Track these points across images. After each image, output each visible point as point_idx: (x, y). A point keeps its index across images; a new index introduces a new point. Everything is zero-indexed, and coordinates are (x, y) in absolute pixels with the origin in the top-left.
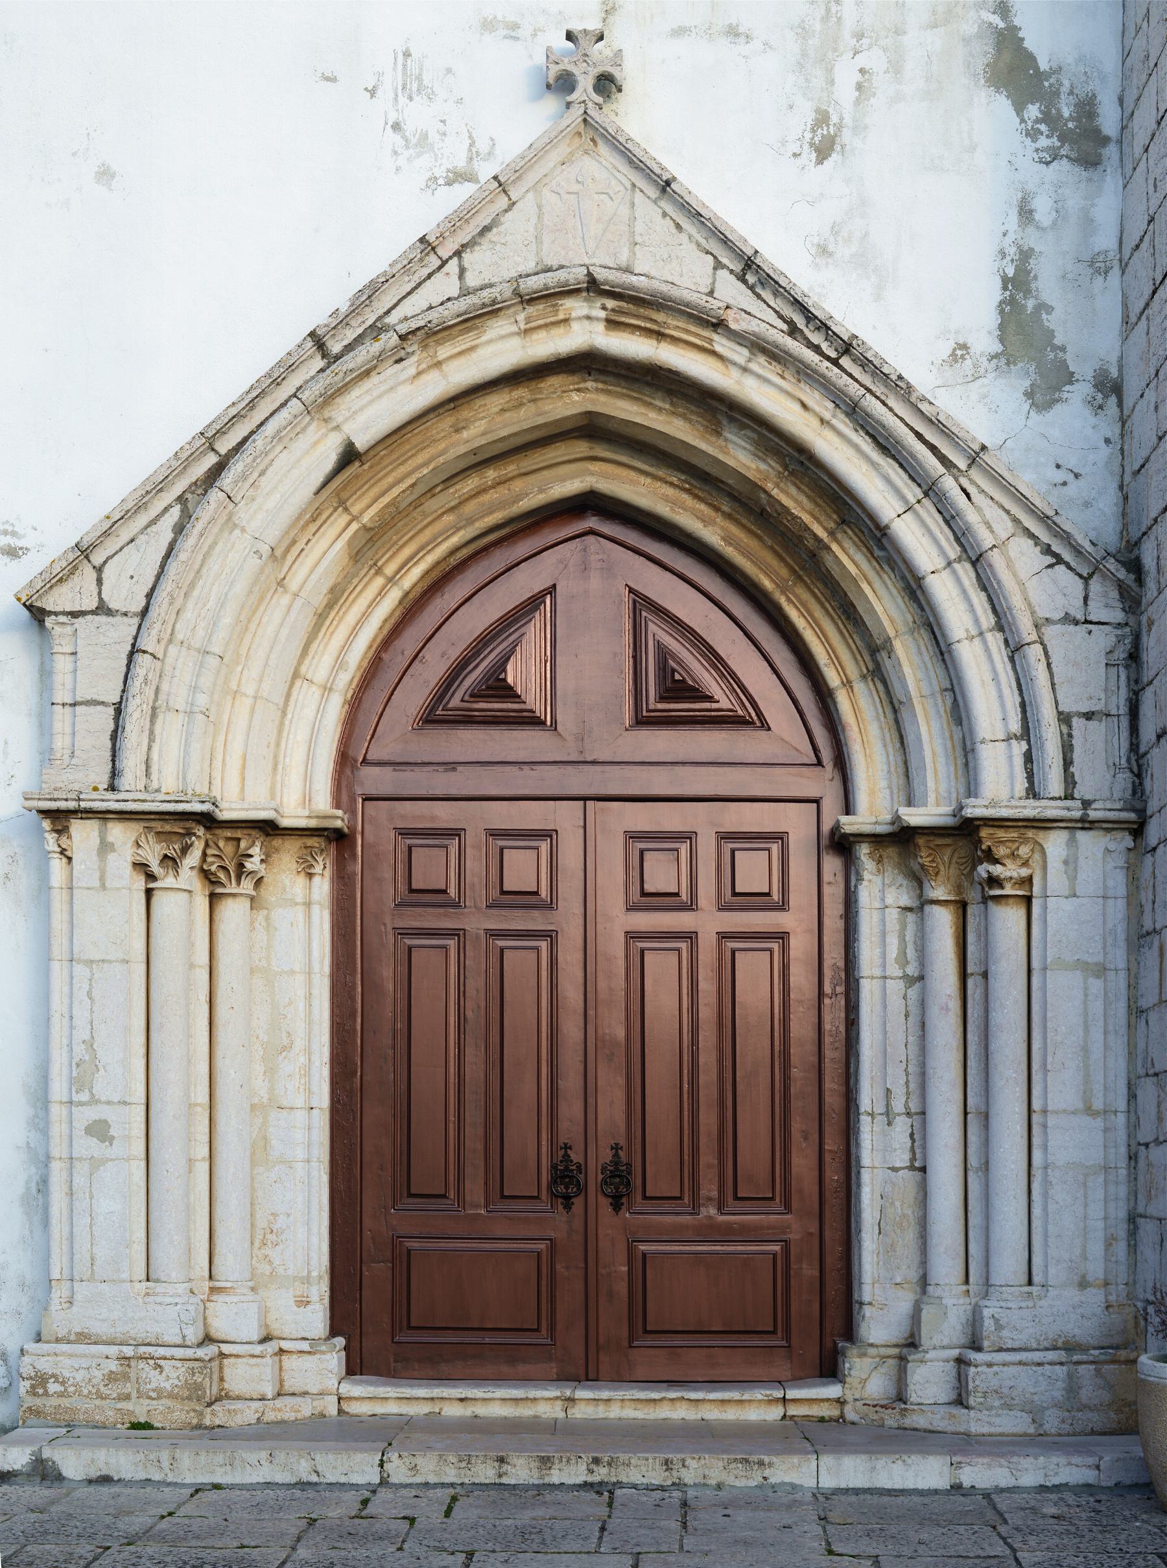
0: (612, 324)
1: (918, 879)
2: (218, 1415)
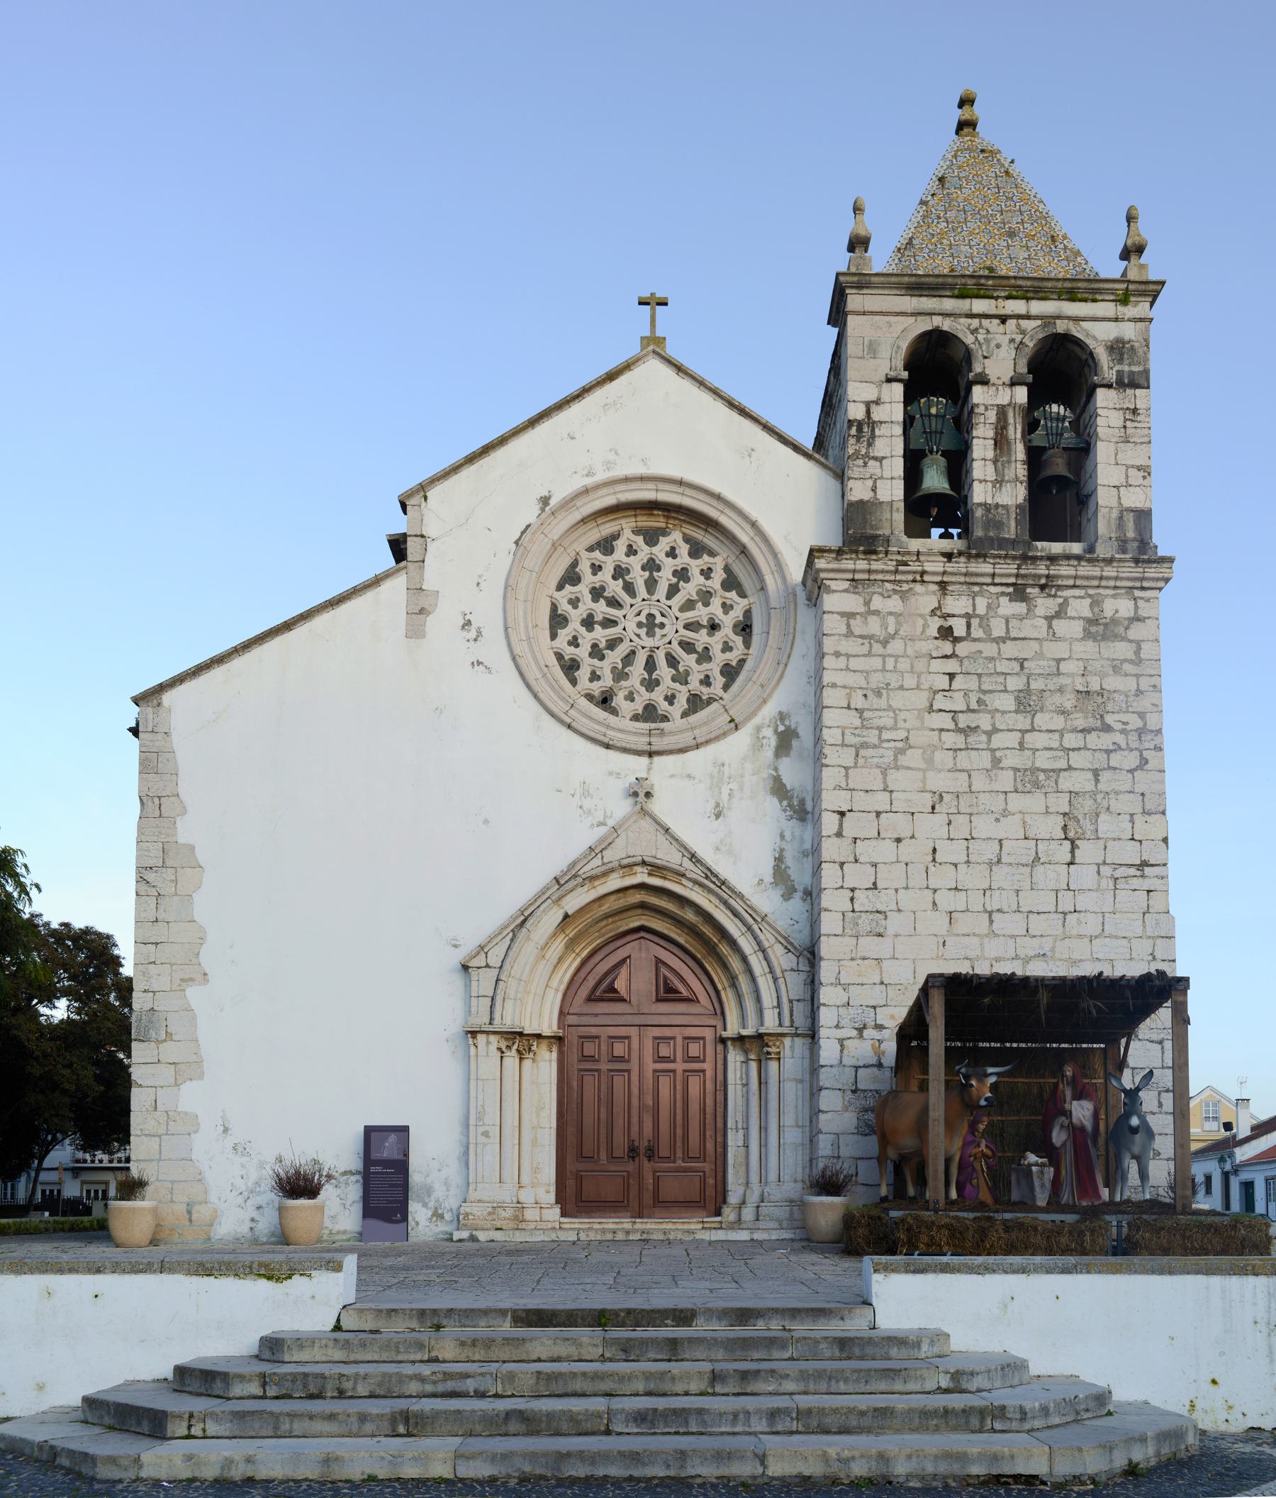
0: (650, 874)
1: (746, 1052)
2: (523, 1225)
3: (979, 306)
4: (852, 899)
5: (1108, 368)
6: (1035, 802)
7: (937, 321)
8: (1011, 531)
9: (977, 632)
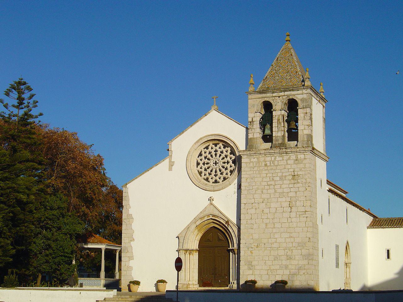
3: (274, 95)
6: (284, 199)
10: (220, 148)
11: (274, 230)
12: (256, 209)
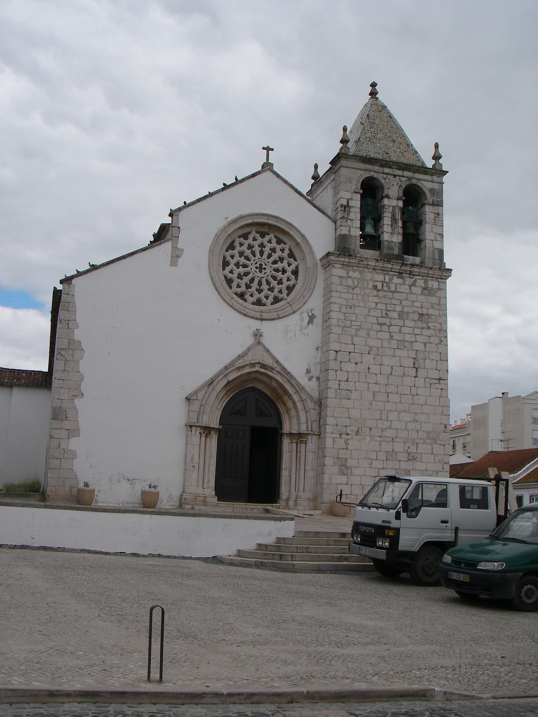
0: (260, 368)
3: (387, 170)
4: (339, 385)
5: (430, 199)
6: (404, 353)
7: (372, 174)
8: (396, 251)
9: (386, 289)
10: (270, 242)
11: (389, 407)
12: (356, 363)
